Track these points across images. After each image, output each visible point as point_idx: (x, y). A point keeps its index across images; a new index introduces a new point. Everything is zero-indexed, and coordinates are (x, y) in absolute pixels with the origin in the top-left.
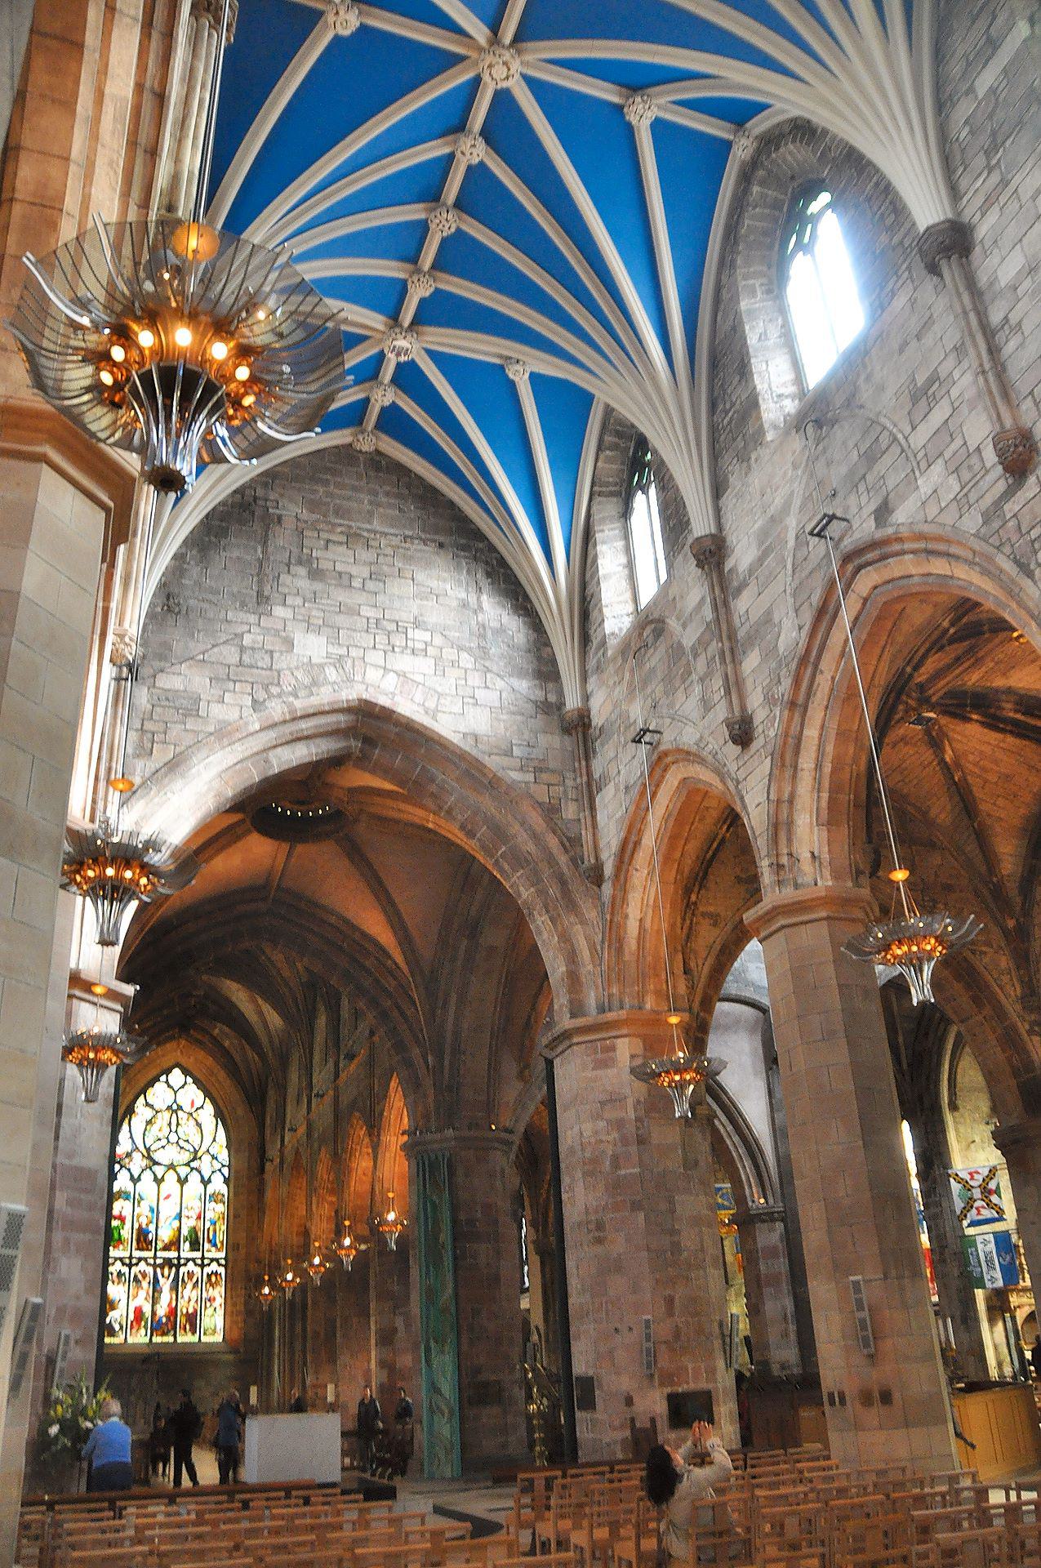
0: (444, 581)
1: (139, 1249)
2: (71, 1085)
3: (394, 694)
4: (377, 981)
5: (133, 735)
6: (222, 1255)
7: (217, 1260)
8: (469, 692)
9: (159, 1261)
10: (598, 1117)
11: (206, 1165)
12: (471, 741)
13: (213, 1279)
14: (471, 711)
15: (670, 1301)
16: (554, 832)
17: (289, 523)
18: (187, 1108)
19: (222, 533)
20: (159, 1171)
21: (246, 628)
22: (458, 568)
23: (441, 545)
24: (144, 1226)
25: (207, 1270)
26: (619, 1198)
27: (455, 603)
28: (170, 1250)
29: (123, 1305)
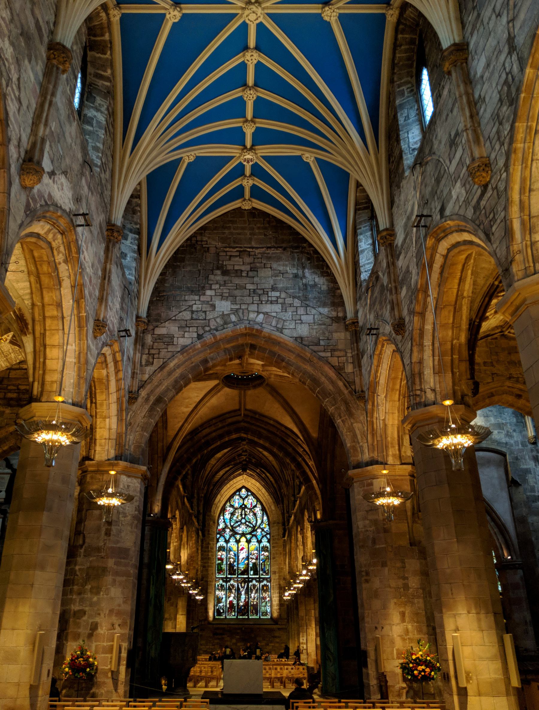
0: (286, 266)
1: (229, 574)
3: (262, 323)
4: (294, 449)
5: (145, 357)
7: (266, 579)
8: (298, 317)
10: (365, 518)
12: (299, 340)
14: (299, 327)
16: (341, 380)
17: (213, 250)
18: (249, 506)
19: (183, 260)
20: (238, 537)
21: (194, 302)
22: (293, 259)
23: (285, 249)
25: (262, 584)
27: (291, 276)
28: (244, 575)
29: (224, 600)
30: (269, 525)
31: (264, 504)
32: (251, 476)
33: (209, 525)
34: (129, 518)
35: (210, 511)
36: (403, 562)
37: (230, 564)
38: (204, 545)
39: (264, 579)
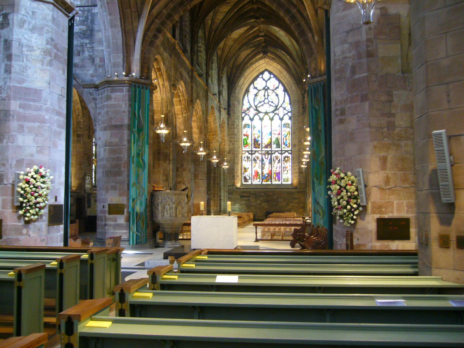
1: (255, 147)
2: (17, 43)
6: (290, 149)
7: (287, 151)
9: (263, 152)
10: (343, 42)
11: (281, 112)
13: (286, 159)
15: (384, 160)
18: (271, 88)
20: (261, 115)
24: (257, 138)
25: (284, 155)
26: (355, 94)
28: (268, 148)
30: (290, 104)
31: (286, 85)
32: (273, 59)
33: (234, 104)
34: (38, 52)
35: (235, 93)
36: (390, 94)
37: (255, 140)
38: (230, 122)
39: (286, 151)
